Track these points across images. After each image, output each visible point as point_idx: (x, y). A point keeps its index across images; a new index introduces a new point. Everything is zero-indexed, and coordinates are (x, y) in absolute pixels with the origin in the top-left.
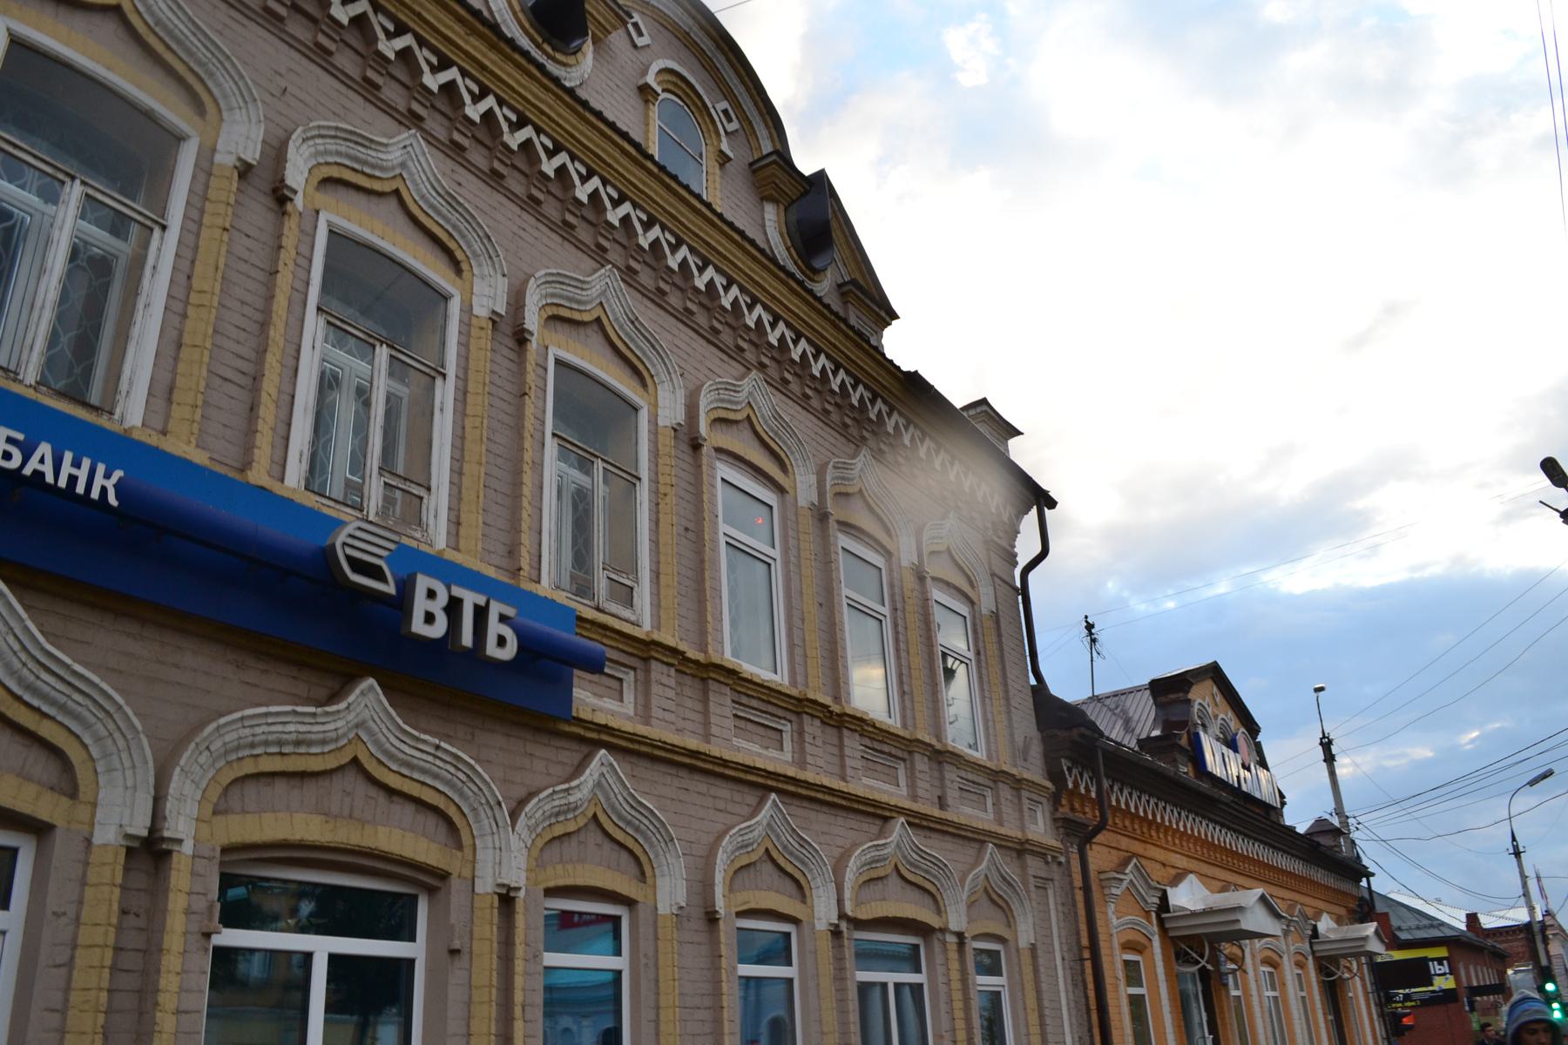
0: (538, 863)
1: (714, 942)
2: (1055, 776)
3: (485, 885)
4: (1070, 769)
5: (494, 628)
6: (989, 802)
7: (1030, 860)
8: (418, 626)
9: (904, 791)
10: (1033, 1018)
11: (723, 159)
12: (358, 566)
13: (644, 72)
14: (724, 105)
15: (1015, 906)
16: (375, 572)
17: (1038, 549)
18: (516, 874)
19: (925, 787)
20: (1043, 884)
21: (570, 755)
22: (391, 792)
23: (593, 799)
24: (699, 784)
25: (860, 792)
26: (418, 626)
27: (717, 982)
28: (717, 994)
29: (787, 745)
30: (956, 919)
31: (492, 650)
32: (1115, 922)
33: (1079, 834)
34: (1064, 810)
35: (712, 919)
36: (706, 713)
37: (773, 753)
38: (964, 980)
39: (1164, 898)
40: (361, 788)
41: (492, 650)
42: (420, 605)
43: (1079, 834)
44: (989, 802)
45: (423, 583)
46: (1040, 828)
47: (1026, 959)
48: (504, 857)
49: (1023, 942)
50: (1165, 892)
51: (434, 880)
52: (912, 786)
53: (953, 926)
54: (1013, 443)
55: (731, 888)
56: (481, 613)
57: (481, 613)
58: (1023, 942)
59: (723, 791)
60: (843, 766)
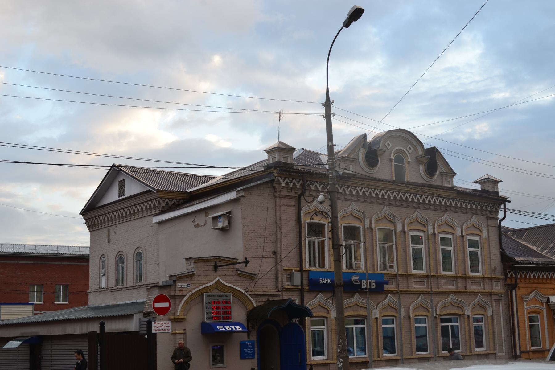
0: (381, 313)
1: (410, 321)
2: (506, 275)
3: (373, 317)
4: (509, 272)
5: (372, 284)
6: (482, 284)
7: (493, 296)
8: (363, 287)
9: (455, 287)
10: (491, 331)
11: (409, 162)
12: (355, 281)
13: (390, 156)
14: (410, 146)
15: (487, 307)
16: (357, 282)
17: (503, 216)
18: (377, 315)
19: (460, 285)
20: (498, 301)
21: (384, 296)
22: (360, 307)
23: (388, 302)
24: (407, 295)
25: (442, 290)
26: (363, 287)
27: (410, 327)
28: (410, 329)
29: (425, 284)
30: (468, 311)
31: (372, 287)
32: (526, 307)
33: (512, 287)
34: (509, 282)
35: (409, 318)
36: (408, 283)
37: (422, 286)
38: (469, 324)
39: (548, 299)
40: (357, 307)
41: (372, 287)
42: (363, 284)
43: (512, 287)
44: (482, 284)
45: (363, 281)
46: (498, 287)
47: (490, 319)
48: (376, 313)
49: (489, 315)
50: (549, 298)
51: (366, 317)
52: (457, 285)
53: (466, 313)
54: (500, 185)
55: (413, 312)
56: (370, 282)
57: (370, 282)
58: (489, 315)
59: (412, 296)
60: (438, 285)
